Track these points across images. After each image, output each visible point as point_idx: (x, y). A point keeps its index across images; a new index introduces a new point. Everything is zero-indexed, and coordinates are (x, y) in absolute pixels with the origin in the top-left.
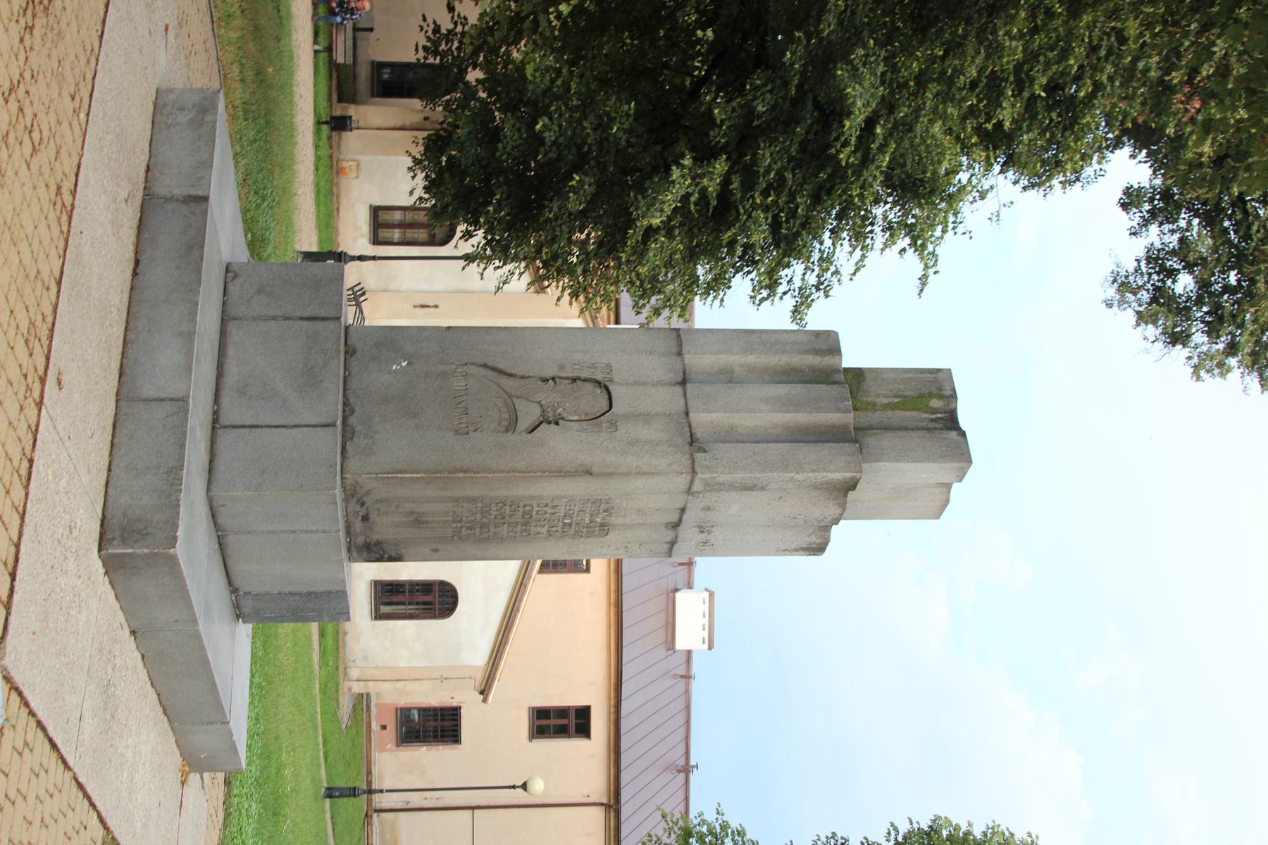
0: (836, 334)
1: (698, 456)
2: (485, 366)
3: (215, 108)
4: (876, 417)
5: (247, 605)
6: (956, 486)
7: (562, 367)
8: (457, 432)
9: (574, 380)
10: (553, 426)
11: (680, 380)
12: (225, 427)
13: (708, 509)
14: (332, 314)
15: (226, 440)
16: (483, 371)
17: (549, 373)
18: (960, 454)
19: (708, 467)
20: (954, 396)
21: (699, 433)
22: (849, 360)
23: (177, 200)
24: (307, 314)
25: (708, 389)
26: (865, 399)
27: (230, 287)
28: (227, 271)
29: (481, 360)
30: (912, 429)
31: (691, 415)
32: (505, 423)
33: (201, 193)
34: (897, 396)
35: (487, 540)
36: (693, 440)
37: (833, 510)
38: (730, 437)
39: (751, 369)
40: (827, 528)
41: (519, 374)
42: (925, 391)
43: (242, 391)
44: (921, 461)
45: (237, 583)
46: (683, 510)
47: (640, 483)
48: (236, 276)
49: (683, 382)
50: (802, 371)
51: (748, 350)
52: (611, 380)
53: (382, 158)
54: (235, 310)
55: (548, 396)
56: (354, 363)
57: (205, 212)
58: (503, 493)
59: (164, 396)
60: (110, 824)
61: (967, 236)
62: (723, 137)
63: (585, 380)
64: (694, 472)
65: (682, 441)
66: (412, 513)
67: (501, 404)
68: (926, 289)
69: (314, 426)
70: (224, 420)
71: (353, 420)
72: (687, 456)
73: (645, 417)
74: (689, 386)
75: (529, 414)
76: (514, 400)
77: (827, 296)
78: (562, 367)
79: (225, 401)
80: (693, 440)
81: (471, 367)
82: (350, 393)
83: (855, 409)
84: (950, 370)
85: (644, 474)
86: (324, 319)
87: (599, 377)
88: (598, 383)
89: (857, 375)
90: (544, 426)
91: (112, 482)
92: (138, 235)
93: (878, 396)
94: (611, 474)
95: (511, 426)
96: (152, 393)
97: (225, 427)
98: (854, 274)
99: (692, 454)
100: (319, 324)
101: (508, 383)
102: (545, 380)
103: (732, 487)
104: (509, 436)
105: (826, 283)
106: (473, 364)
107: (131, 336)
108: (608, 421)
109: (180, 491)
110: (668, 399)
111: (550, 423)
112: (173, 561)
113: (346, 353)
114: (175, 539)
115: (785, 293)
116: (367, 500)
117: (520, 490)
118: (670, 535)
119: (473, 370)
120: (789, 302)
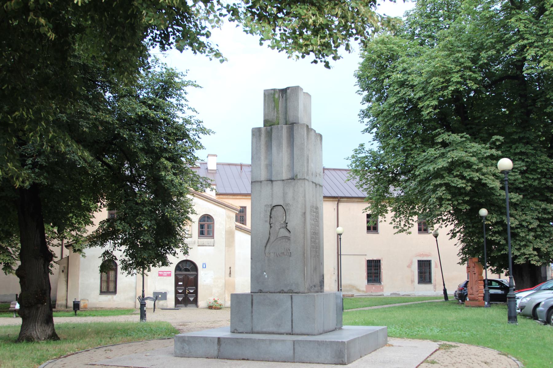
0: (253, 129)
1: (299, 177)
2: (266, 247)
3: (182, 337)
4: (281, 116)
5: (338, 326)
6: (304, 91)
7: (266, 221)
8: (290, 256)
9: (270, 217)
10: (288, 225)
11: (271, 182)
12: (292, 331)
13: (312, 174)
14: (251, 297)
15: (296, 330)
16: (268, 247)
17: (268, 226)
18: (296, 89)
19: (303, 174)
20: (274, 90)
21: (290, 177)
22: (261, 125)
23: (220, 347)
24: (250, 305)
25: (274, 173)
26: (275, 120)
27: (240, 331)
28: (234, 332)
29: (263, 248)
30: (286, 105)
31: (284, 179)
32: (287, 240)
33: (217, 340)
34: (274, 109)
35: (319, 246)
36: (293, 179)
37: (313, 133)
38: (291, 166)
39: (266, 158)
40: (316, 134)
41: (269, 235)
42: (272, 99)
43: (279, 326)
44: (298, 103)
45: (334, 328)
46: (313, 182)
47: (307, 197)
48: (236, 330)
49: (272, 181)
50: (266, 141)
51: (259, 159)
52: (271, 205)
53: (79, 290)
54: (249, 329)
55: (277, 226)
56: (265, 290)
57: (224, 338)
58: (309, 241)
59: (293, 348)
60: (422, 361)
61: (188, 71)
62: (150, 159)
63: (271, 214)
64: (304, 179)
65: (293, 182)
66: (314, 271)
67: (280, 242)
68: (200, 85)
69: (292, 302)
70: (290, 331)
71: (286, 290)
72: (299, 181)
73: (285, 194)
74: (273, 179)
75: (283, 232)
76: (278, 237)
77: (202, 122)
78: (266, 221)
79: (283, 331)
80: (293, 179)
81: (266, 251)
82: (276, 291)
83: (278, 124)
84: (264, 90)
85: (305, 195)
86: (252, 300)
87: (270, 209)
88: (272, 209)
89: (266, 122)
90: (288, 228)
91: (323, 362)
92: (234, 359)
93: (274, 115)
94: (305, 206)
95: (288, 238)
96: (292, 352)
97: (292, 331)
98: (197, 112)
99: (298, 179)
100: (254, 301)
101: (272, 239)
102: (271, 227)
103: (308, 166)
104: (292, 239)
105: (197, 122)
106: (265, 251)
107: (271, 359)
108: (286, 206)
109: (326, 341)
110: (278, 187)
111: (287, 226)
112: (348, 342)
113: (261, 293)
114: (342, 342)
115: (198, 137)
116: (311, 285)
117: (309, 235)
118: (318, 186)
119: (267, 250)
120: (201, 135)
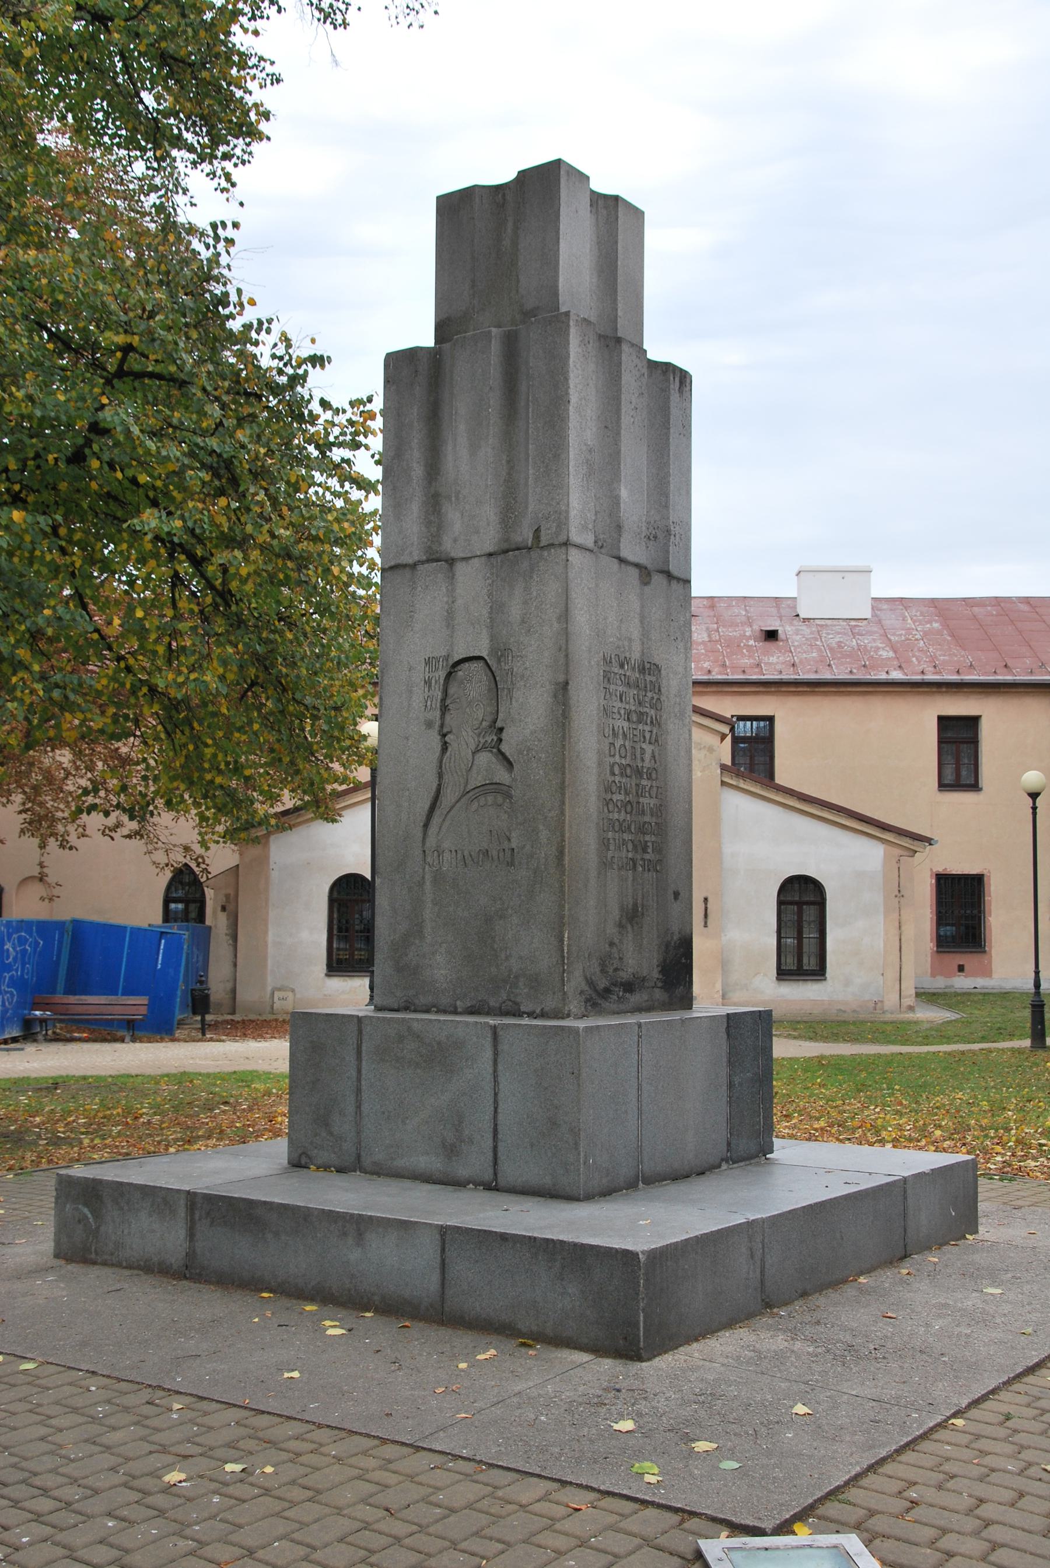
2: (426, 826)
10: (504, 735)
12: (495, 1174)
16: (433, 829)
22: (427, 339)
32: (500, 799)
52: (447, 658)
53: (270, 962)
55: (464, 741)
66: (621, 926)
69: (496, 1054)
70: (488, 1176)
76: (470, 787)
78: (429, 724)
81: (428, 844)
87: (442, 674)
88: (449, 675)
90: (504, 747)
96: (436, 1277)
97: (495, 1174)
101: (449, 797)
102: (445, 747)
108: (499, 661)
111: (500, 740)
112: (658, 1256)
119: (431, 841)
